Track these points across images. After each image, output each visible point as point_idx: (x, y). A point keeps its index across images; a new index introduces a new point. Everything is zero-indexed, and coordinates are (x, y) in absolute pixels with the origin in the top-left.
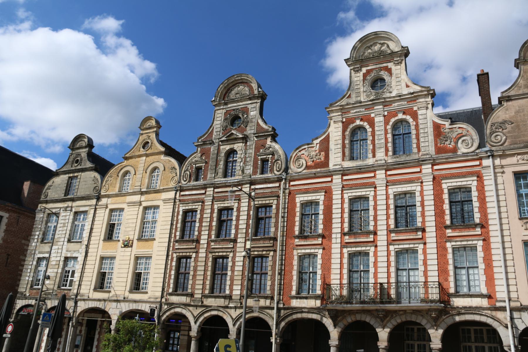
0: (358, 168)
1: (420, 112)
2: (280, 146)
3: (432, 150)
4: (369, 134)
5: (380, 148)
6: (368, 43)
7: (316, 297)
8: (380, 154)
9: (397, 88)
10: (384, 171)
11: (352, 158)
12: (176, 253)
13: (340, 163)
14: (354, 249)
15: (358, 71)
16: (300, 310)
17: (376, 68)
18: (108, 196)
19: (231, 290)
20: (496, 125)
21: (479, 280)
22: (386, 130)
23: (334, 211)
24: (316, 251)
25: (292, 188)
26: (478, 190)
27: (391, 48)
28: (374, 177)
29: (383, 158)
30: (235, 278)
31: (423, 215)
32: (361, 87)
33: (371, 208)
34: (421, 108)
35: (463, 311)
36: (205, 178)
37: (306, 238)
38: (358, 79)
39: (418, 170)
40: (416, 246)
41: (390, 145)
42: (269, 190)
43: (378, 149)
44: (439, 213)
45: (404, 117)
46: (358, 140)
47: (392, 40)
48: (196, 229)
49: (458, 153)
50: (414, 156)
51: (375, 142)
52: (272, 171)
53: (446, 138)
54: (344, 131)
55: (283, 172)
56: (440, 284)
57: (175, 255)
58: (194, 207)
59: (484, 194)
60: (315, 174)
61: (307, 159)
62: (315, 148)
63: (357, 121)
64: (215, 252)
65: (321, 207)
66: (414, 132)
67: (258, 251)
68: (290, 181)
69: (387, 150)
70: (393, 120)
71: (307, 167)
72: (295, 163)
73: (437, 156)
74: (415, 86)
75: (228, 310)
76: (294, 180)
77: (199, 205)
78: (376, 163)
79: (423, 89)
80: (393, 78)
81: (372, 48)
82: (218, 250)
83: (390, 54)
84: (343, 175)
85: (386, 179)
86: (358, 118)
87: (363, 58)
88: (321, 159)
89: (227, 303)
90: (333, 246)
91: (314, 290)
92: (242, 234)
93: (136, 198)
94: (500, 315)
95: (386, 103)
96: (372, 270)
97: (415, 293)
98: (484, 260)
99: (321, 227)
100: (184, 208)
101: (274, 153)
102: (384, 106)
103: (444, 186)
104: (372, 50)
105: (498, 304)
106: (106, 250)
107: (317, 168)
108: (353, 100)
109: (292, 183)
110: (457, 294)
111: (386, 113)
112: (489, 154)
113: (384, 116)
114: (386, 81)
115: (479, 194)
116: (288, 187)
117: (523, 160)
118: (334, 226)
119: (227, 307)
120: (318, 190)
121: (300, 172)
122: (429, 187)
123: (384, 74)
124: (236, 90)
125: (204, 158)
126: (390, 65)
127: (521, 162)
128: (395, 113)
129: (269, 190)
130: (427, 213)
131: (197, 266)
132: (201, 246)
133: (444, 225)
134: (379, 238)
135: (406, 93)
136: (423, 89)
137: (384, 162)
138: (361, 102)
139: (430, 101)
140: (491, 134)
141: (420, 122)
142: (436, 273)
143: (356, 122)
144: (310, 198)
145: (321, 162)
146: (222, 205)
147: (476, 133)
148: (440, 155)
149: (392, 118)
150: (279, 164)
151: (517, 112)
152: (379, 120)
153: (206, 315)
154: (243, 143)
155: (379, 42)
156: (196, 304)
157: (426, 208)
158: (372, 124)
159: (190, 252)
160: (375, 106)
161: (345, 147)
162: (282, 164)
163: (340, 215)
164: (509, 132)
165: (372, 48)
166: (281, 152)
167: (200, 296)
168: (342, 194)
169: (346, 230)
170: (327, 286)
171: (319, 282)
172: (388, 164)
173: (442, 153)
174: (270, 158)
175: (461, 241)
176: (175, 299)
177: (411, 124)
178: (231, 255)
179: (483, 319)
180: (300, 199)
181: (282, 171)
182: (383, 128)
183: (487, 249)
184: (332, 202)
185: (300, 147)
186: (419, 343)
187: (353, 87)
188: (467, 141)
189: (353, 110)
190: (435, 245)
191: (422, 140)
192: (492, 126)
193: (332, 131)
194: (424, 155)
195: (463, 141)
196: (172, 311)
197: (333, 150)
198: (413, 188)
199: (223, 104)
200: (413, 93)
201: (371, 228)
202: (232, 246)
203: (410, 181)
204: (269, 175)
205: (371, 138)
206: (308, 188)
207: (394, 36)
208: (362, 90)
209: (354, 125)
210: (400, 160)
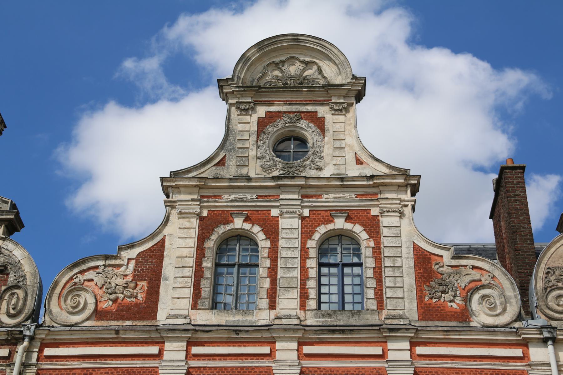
0: (233, 328)
1: (385, 221)
2: (26, 253)
3: (410, 310)
4: (264, 253)
5: (288, 288)
6: (276, 57)
9: (334, 163)
10: (294, 345)
11: (214, 306)
13: (185, 312)
15: (246, 110)
17: (290, 112)
20: (557, 273)
25: (47, 365)
27: (326, 75)
28: (270, 355)
29: (293, 313)
32: (251, 147)
34: (388, 211)
38: (247, 127)
39: (378, 350)
41: (312, 284)
43: (282, 290)
45: (348, 226)
46: (233, 265)
47: (331, 60)
49: (472, 324)
50: (368, 316)
51: (276, 273)
53: (445, 287)
54: (202, 238)
55: (27, 320)
60: (117, 332)
61: (100, 292)
62: (123, 268)
63: (236, 220)
66: (370, 263)
68: (44, 345)
69: (304, 297)
70: (322, 229)
72: (65, 301)
73: (423, 323)
74: (376, 163)
76: (56, 345)
78: (277, 322)
79: (394, 173)
80: (326, 138)
81: (283, 68)
83: (323, 86)
84: (191, 343)
85: (300, 363)
86: (240, 213)
87: (262, 85)
88: (136, 297)
101: (6, 268)
102: (302, 196)
104: (282, 72)
107: (123, 319)
108: (231, 170)
109: (48, 352)
111: (306, 213)
112: (546, 334)
113: (303, 218)
114: (310, 145)
116: (34, 360)
121: (76, 325)
126: (322, 111)
128: (327, 214)
135: (356, 174)
136: (394, 173)
137: (296, 322)
138: (249, 179)
139: (409, 200)
140: (548, 290)
141: (386, 242)
143: (233, 221)
145: (137, 305)
147: (512, 284)
148: (430, 323)
149: (319, 225)
150: (18, 299)
155: (302, 59)
160: (282, 193)
161: (202, 277)
162: (25, 299)
165: (283, 68)
166: (27, 268)
172: (307, 328)
173: (433, 319)
177: (364, 244)
185: (84, 261)
187: (231, 144)
188: (492, 300)
189: (229, 194)
191: (388, 282)
192: (548, 273)
193: (171, 235)
194: (394, 317)
195: (484, 297)
197: (171, 279)
200: (372, 177)
205: (268, 263)
206: (94, 369)
207: (336, 51)
208: (252, 153)
209: (229, 227)
210: (335, 324)
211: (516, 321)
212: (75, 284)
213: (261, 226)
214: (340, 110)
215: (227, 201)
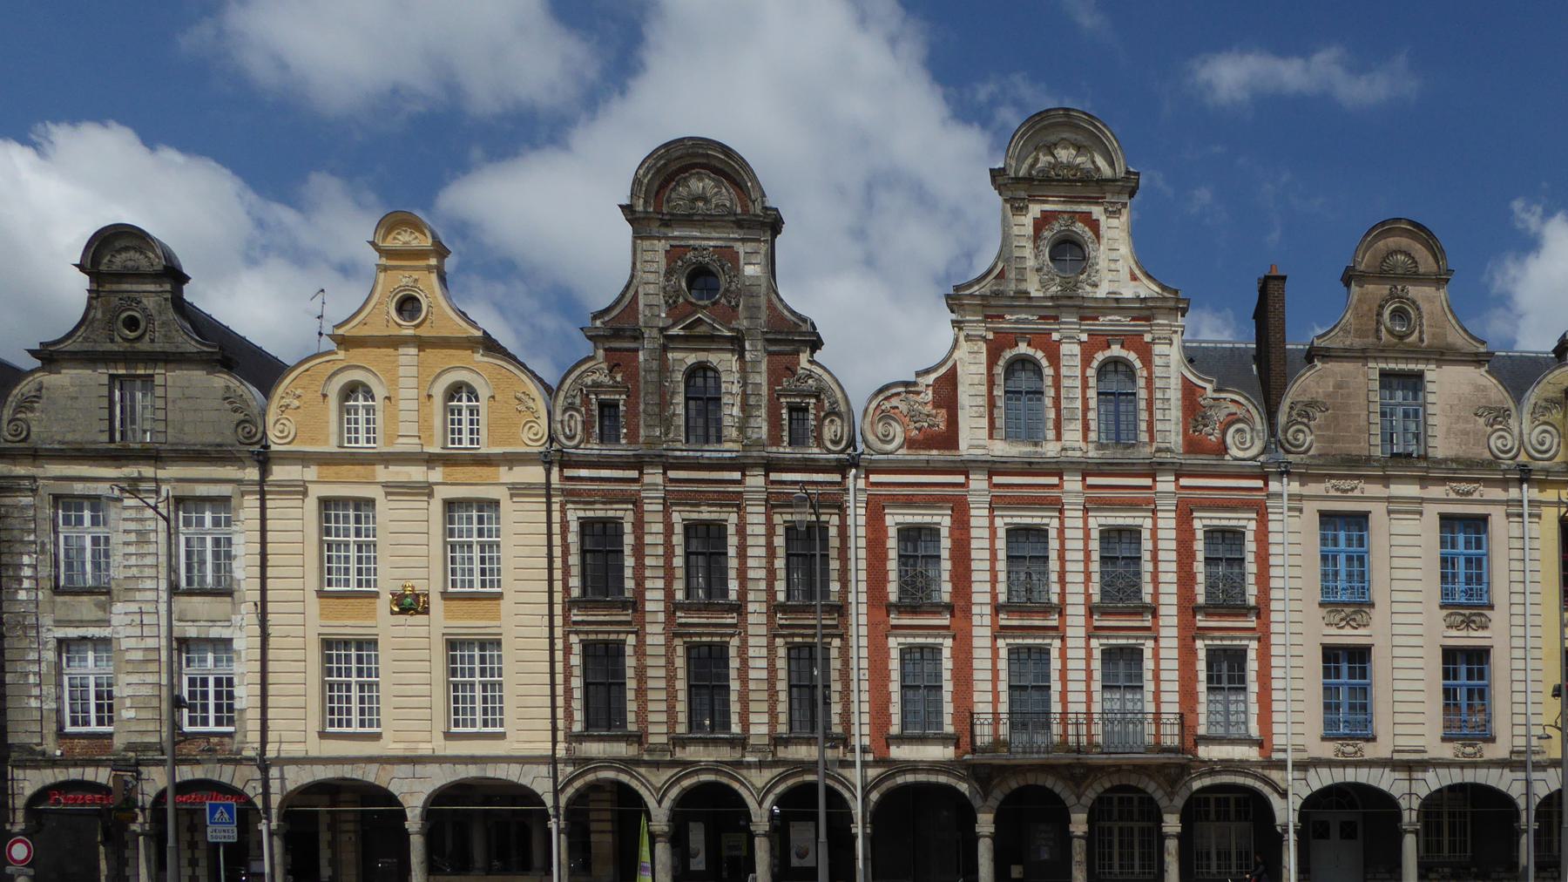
1: (1157, 349)
4: (1049, 381)
7: (944, 740)
8: (1073, 434)
12: (577, 633)
14: (1019, 641)
16: (912, 766)
18: (304, 459)
19: (745, 724)
21: (1245, 712)
22: (1085, 379)
23: (974, 554)
24: (939, 640)
26: (1256, 540)
29: (1077, 445)
30: (752, 696)
31: (1155, 581)
33: (1053, 555)
34: (1159, 338)
35: (1218, 768)
36: (633, 437)
37: (914, 610)
40: (1139, 642)
41: (1092, 415)
42: (820, 490)
44: (1186, 579)
48: (628, 573)
52: (819, 441)
54: (992, 363)
56: (1182, 715)
57: (574, 639)
58: (611, 514)
59: (1267, 550)
62: (922, 395)
64: (691, 635)
65: (946, 543)
67: (803, 636)
69: (1086, 428)
70: (1100, 356)
71: (910, 443)
75: (744, 772)
77: (626, 510)
81: (1055, 152)
82: (699, 630)
84: (991, 474)
89: (735, 755)
90: (976, 631)
91: (940, 725)
92: (759, 593)
93: (416, 473)
94: (1275, 775)
95: (1088, 311)
96: (1056, 686)
97: (1135, 732)
98: (1258, 676)
99: (947, 587)
100: (581, 514)
103: (1197, 524)
105: (1276, 756)
106: (337, 618)
107: (930, 447)
110: (1210, 740)
111: (1084, 337)
115: (1258, 549)
117: (1337, 490)
118: (975, 587)
119: (738, 764)
120: (935, 502)
122: (1168, 522)
123: (1079, 227)
124: (696, 186)
125: (619, 378)
126: (1097, 212)
127: (1333, 493)
129: (820, 490)
130: (1162, 577)
131: (645, 667)
132: (648, 618)
133: (1193, 605)
134: (1069, 621)
137: (1079, 454)
138: (1030, 298)
141: (1158, 372)
142: (1176, 697)
144: (918, 519)
145: (940, 434)
146: (695, 516)
151: (1339, 386)
152: (1070, 350)
153: (686, 783)
154: (732, 351)
156: (656, 758)
157: (1162, 566)
158: (1054, 359)
159: (618, 633)
161: (995, 406)
163: (987, 565)
164: (1319, 427)
167: (664, 739)
168: (992, 518)
169: (1002, 598)
170: (967, 717)
171: (948, 708)
174: (812, 406)
175: (1222, 639)
176: (594, 749)
177: (1139, 373)
178: (735, 642)
179: (1249, 782)
180: (894, 519)
181: (844, 443)
182: (1078, 372)
183: (1265, 656)
184: (969, 532)
186: (1120, 824)
190: (1175, 643)
191: (1158, 415)
195: (1238, 431)
196: (590, 777)
198: (1138, 522)
199: (658, 223)
201: (1055, 599)
202: (735, 621)
203: (1132, 505)
204: (814, 451)
205: (1052, 392)
206: (913, 495)
211: (1262, 453)
212: (883, 411)
213: (1044, 352)
214: (1114, 212)
215: (1009, 322)
